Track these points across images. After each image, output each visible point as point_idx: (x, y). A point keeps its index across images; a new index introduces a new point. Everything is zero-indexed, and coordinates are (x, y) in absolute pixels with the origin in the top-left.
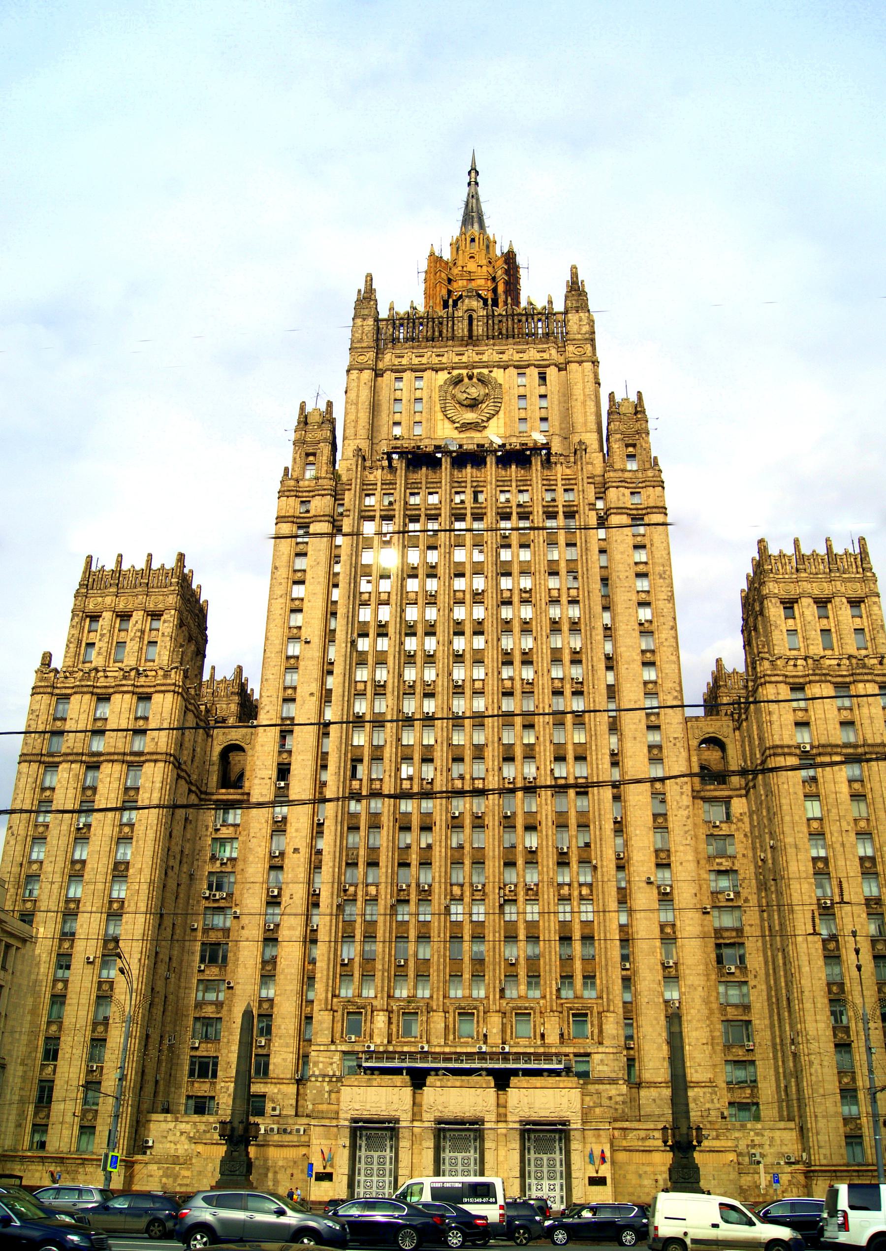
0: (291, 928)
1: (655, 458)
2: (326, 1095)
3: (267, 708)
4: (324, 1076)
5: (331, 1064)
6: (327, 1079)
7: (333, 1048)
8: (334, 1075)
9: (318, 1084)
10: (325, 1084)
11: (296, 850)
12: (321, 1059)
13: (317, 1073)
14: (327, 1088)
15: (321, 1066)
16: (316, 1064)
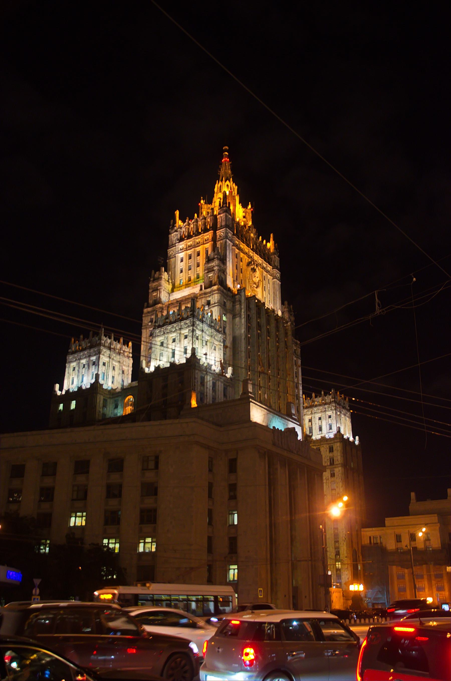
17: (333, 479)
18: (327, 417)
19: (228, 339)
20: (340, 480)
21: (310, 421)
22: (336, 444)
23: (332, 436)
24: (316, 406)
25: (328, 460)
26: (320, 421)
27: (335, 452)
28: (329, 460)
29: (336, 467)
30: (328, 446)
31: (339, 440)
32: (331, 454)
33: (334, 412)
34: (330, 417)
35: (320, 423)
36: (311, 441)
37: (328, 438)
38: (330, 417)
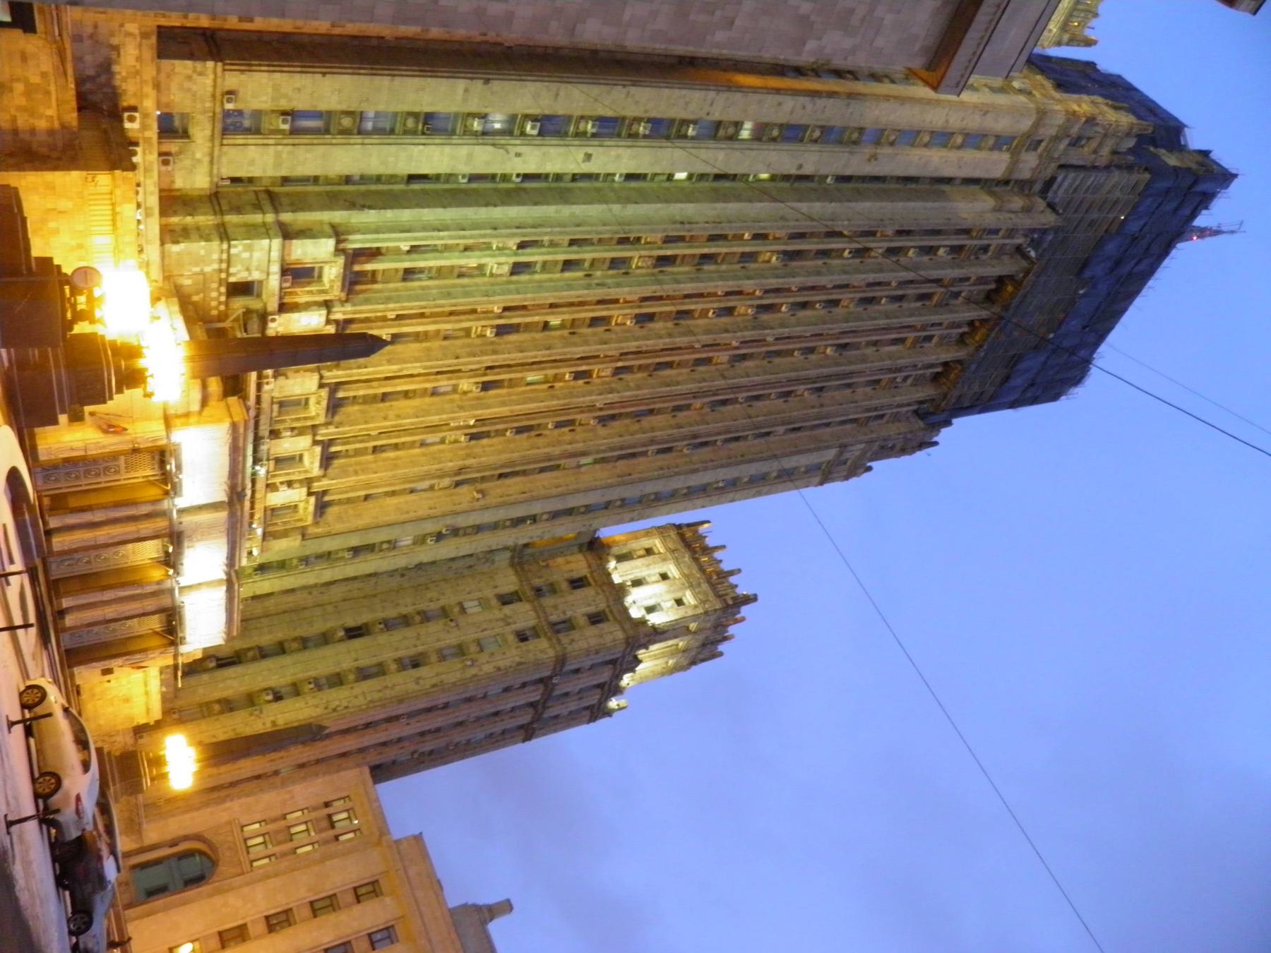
0: (470, 156)
1: (870, 469)
2: (197, 269)
3: (809, 106)
4: (229, 262)
5: (248, 269)
6: (224, 266)
7: (275, 268)
8: (229, 275)
9: (215, 256)
10: (216, 266)
11: (588, 157)
12: (257, 255)
13: (233, 251)
14: (208, 269)
15: (246, 255)
16: (249, 249)
17: (511, 638)
18: (678, 595)
19: (953, 155)
20: (517, 659)
21: (649, 552)
22: (617, 627)
23: (635, 613)
24: (696, 560)
25: (564, 613)
26: (658, 577)
27: (592, 631)
28: (562, 617)
29: (549, 639)
30: (602, 606)
31: (631, 632)
32: (582, 621)
33: (700, 611)
34: (679, 602)
35: (654, 579)
36: (601, 559)
37: (627, 605)
38: (679, 602)
